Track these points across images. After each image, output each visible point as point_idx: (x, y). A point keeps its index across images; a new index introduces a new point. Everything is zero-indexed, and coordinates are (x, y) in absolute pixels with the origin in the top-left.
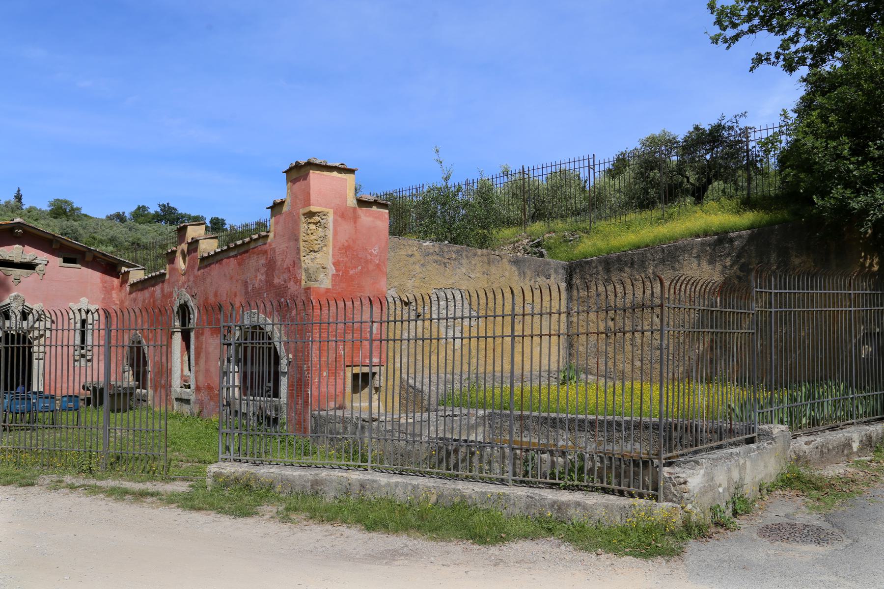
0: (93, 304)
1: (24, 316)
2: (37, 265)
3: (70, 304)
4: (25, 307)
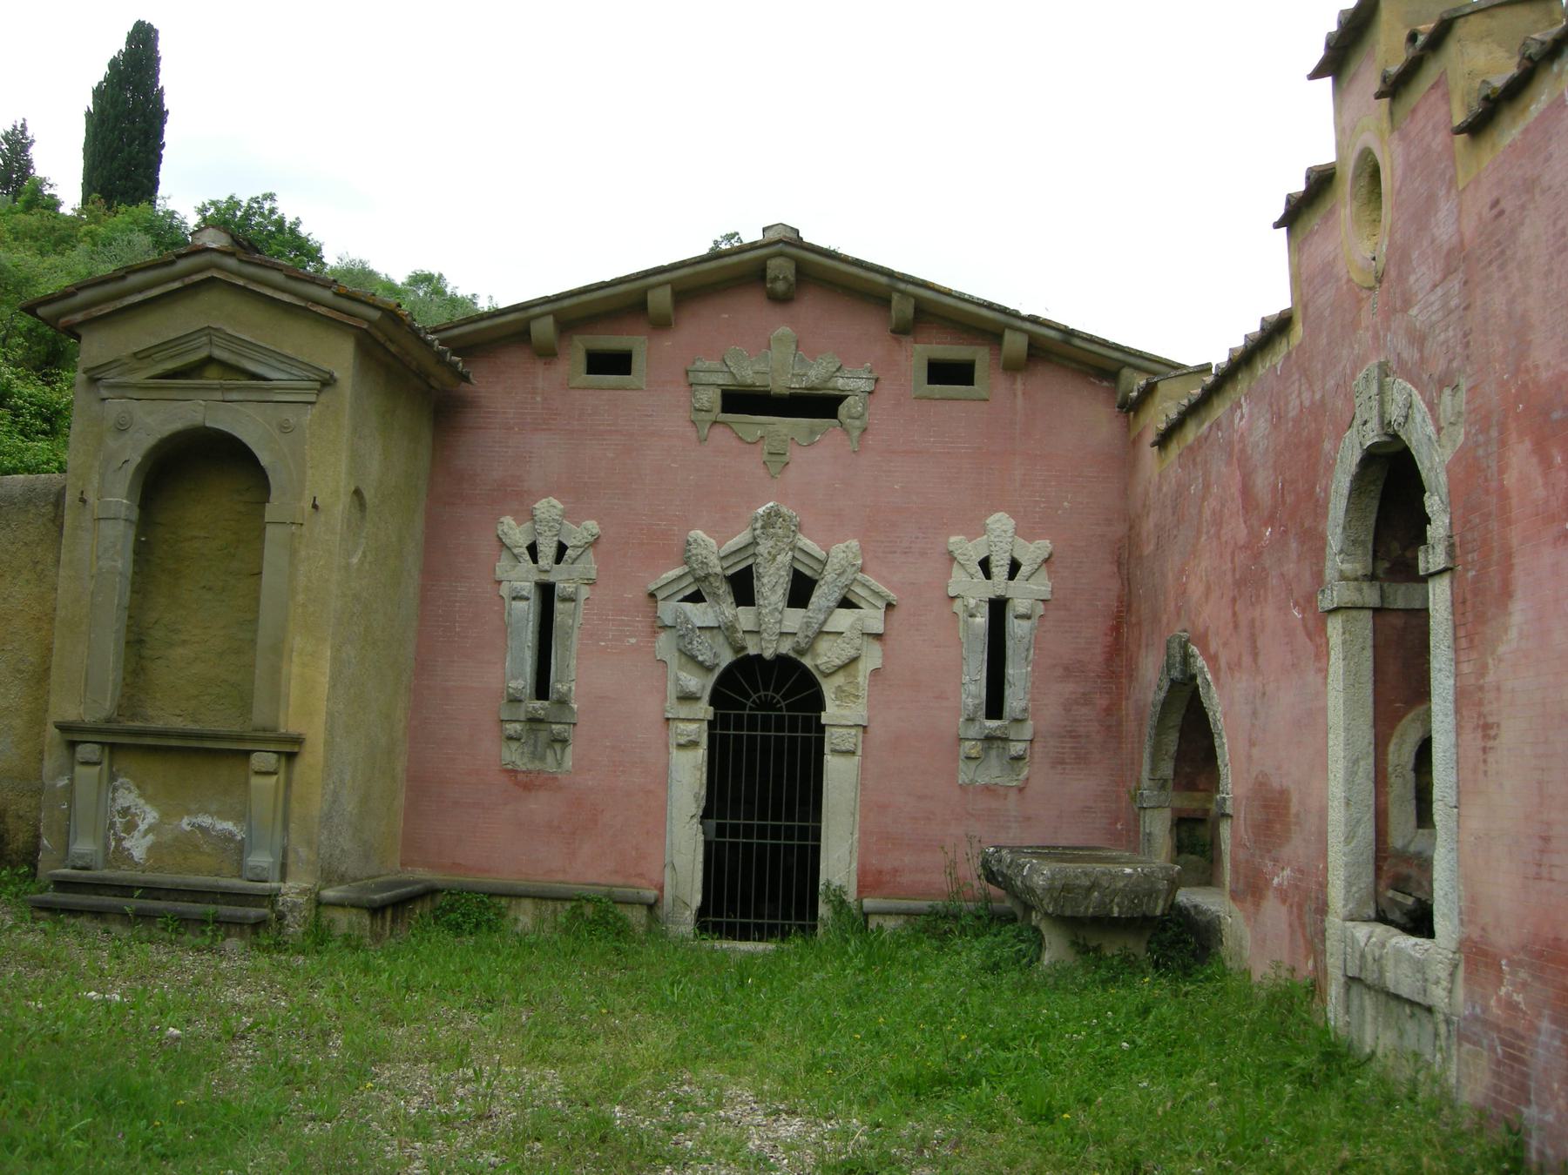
0: (1030, 536)
1: (801, 590)
2: (840, 399)
3: (953, 539)
4: (799, 555)
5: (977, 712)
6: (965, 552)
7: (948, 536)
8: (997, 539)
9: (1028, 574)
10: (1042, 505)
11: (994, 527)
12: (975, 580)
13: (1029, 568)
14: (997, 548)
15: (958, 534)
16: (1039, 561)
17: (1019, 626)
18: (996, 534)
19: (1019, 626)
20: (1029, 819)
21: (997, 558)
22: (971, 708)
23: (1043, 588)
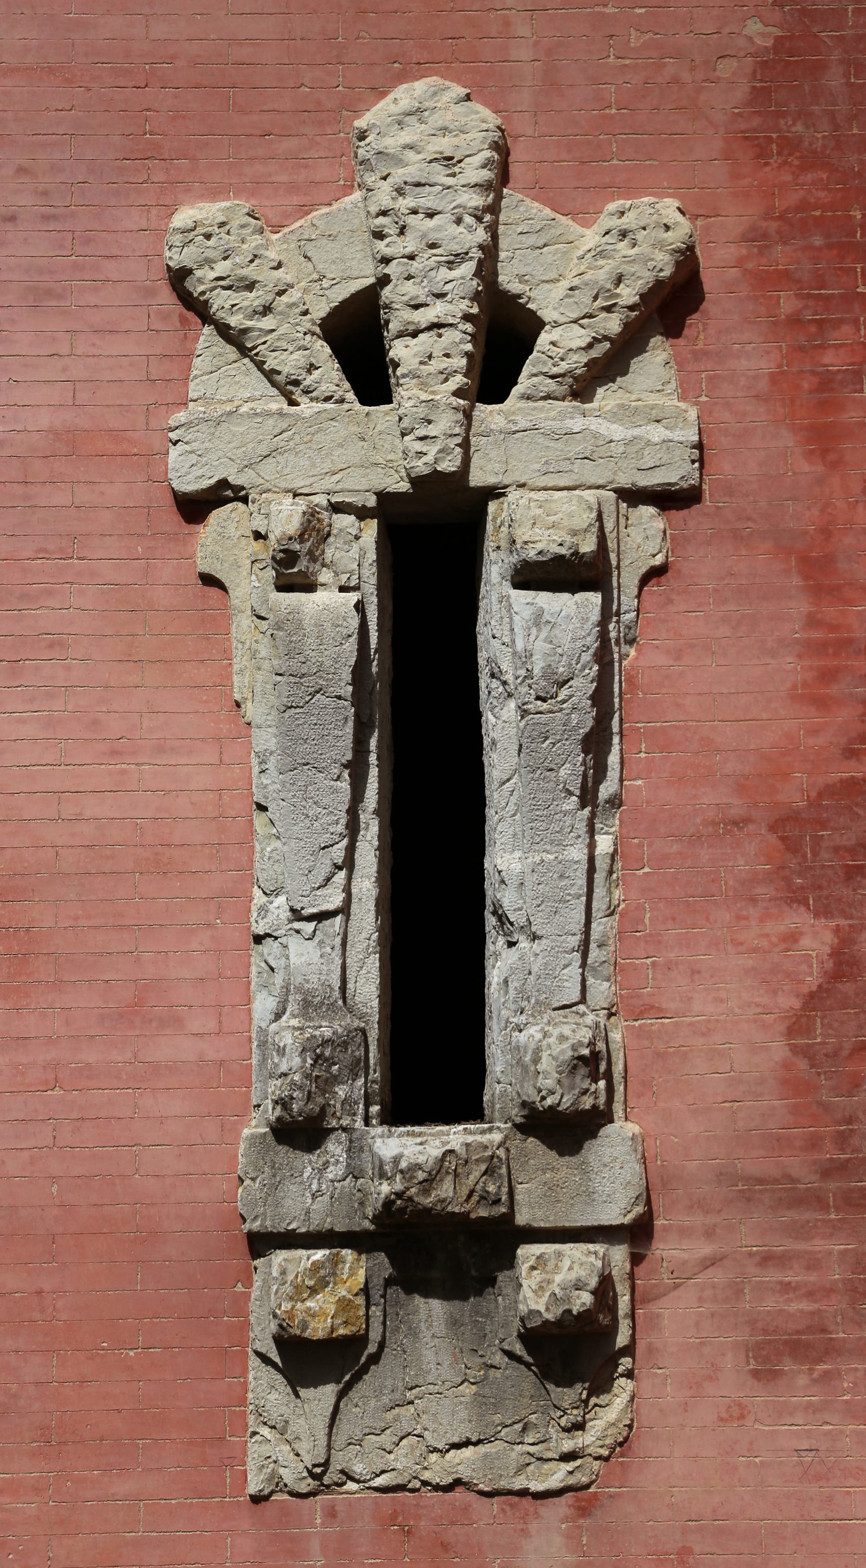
5: (327, 1084)
6: (250, 272)
7: (171, 210)
8: (404, 204)
9: (577, 362)
10: (635, 40)
11: (392, 142)
12: (306, 407)
13: (578, 337)
14: (410, 244)
15: (214, 194)
16: (628, 294)
17: (538, 619)
18: (399, 175)
19: (538, 619)
20: (445, 1547)
21: (411, 289)
22: (292, 1062)
23: (657, 433)
